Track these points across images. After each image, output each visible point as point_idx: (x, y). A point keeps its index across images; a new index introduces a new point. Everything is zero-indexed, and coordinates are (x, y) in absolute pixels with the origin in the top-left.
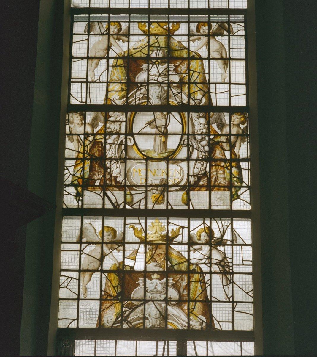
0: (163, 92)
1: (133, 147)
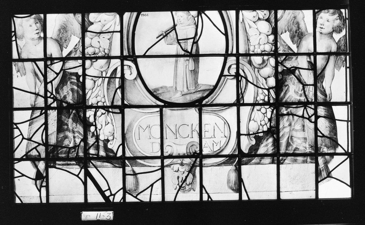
1: (136, 82)
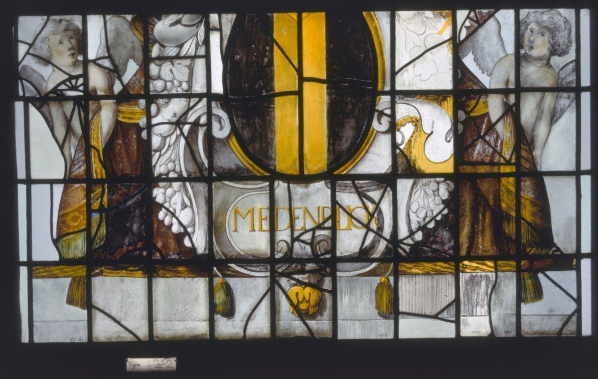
1: (230, 141)
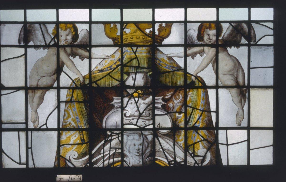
0: (146, 144)
